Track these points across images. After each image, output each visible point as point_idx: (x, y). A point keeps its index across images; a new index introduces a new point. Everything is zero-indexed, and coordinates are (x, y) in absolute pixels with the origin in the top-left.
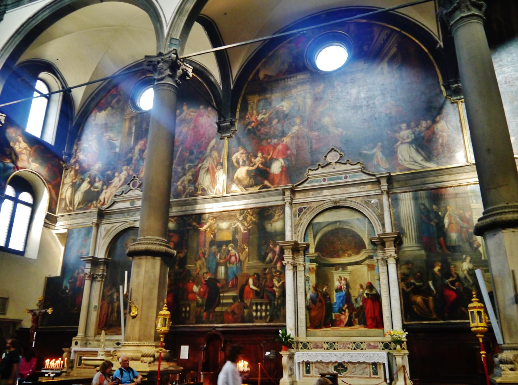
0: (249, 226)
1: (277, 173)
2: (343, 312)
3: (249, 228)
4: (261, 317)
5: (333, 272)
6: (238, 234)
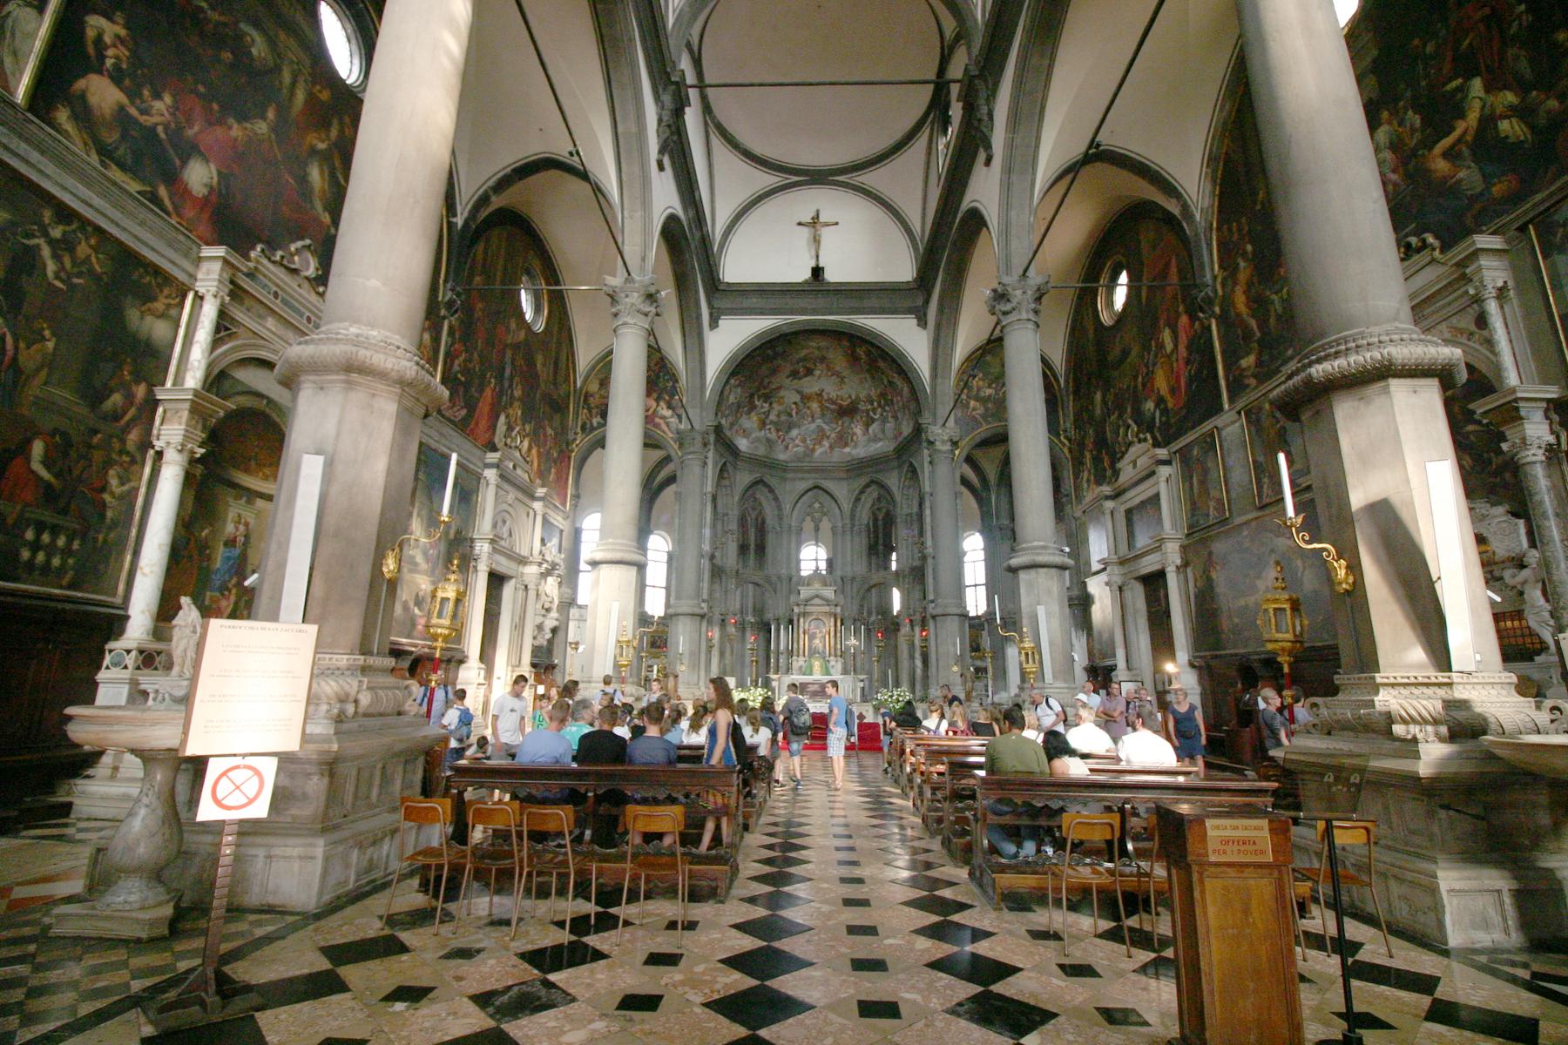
0: (79, 275)
1: (194, 193)
3: (76, 281)
4: (46, 568)
5: (230, 500)
6: (30, 275)
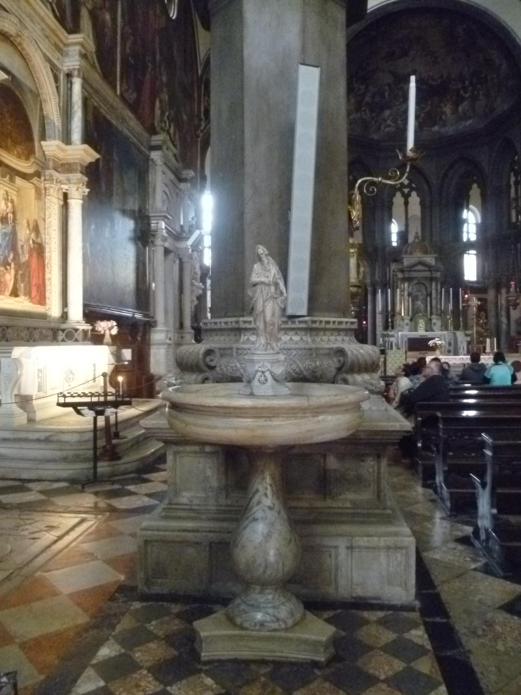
2: (8, 267)
